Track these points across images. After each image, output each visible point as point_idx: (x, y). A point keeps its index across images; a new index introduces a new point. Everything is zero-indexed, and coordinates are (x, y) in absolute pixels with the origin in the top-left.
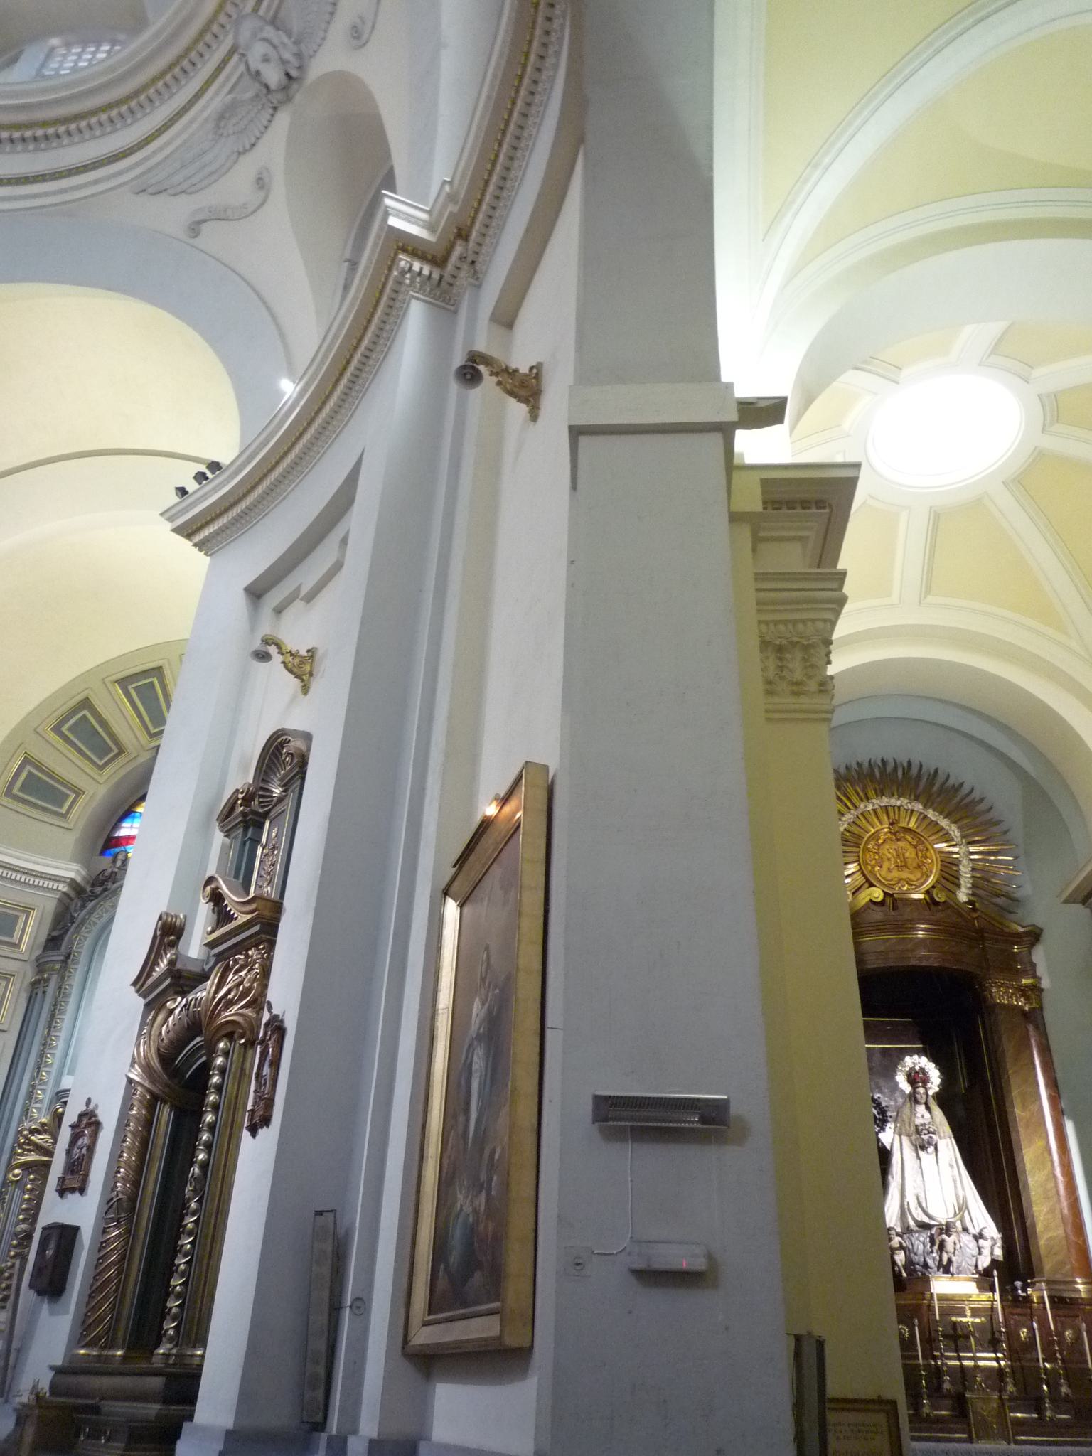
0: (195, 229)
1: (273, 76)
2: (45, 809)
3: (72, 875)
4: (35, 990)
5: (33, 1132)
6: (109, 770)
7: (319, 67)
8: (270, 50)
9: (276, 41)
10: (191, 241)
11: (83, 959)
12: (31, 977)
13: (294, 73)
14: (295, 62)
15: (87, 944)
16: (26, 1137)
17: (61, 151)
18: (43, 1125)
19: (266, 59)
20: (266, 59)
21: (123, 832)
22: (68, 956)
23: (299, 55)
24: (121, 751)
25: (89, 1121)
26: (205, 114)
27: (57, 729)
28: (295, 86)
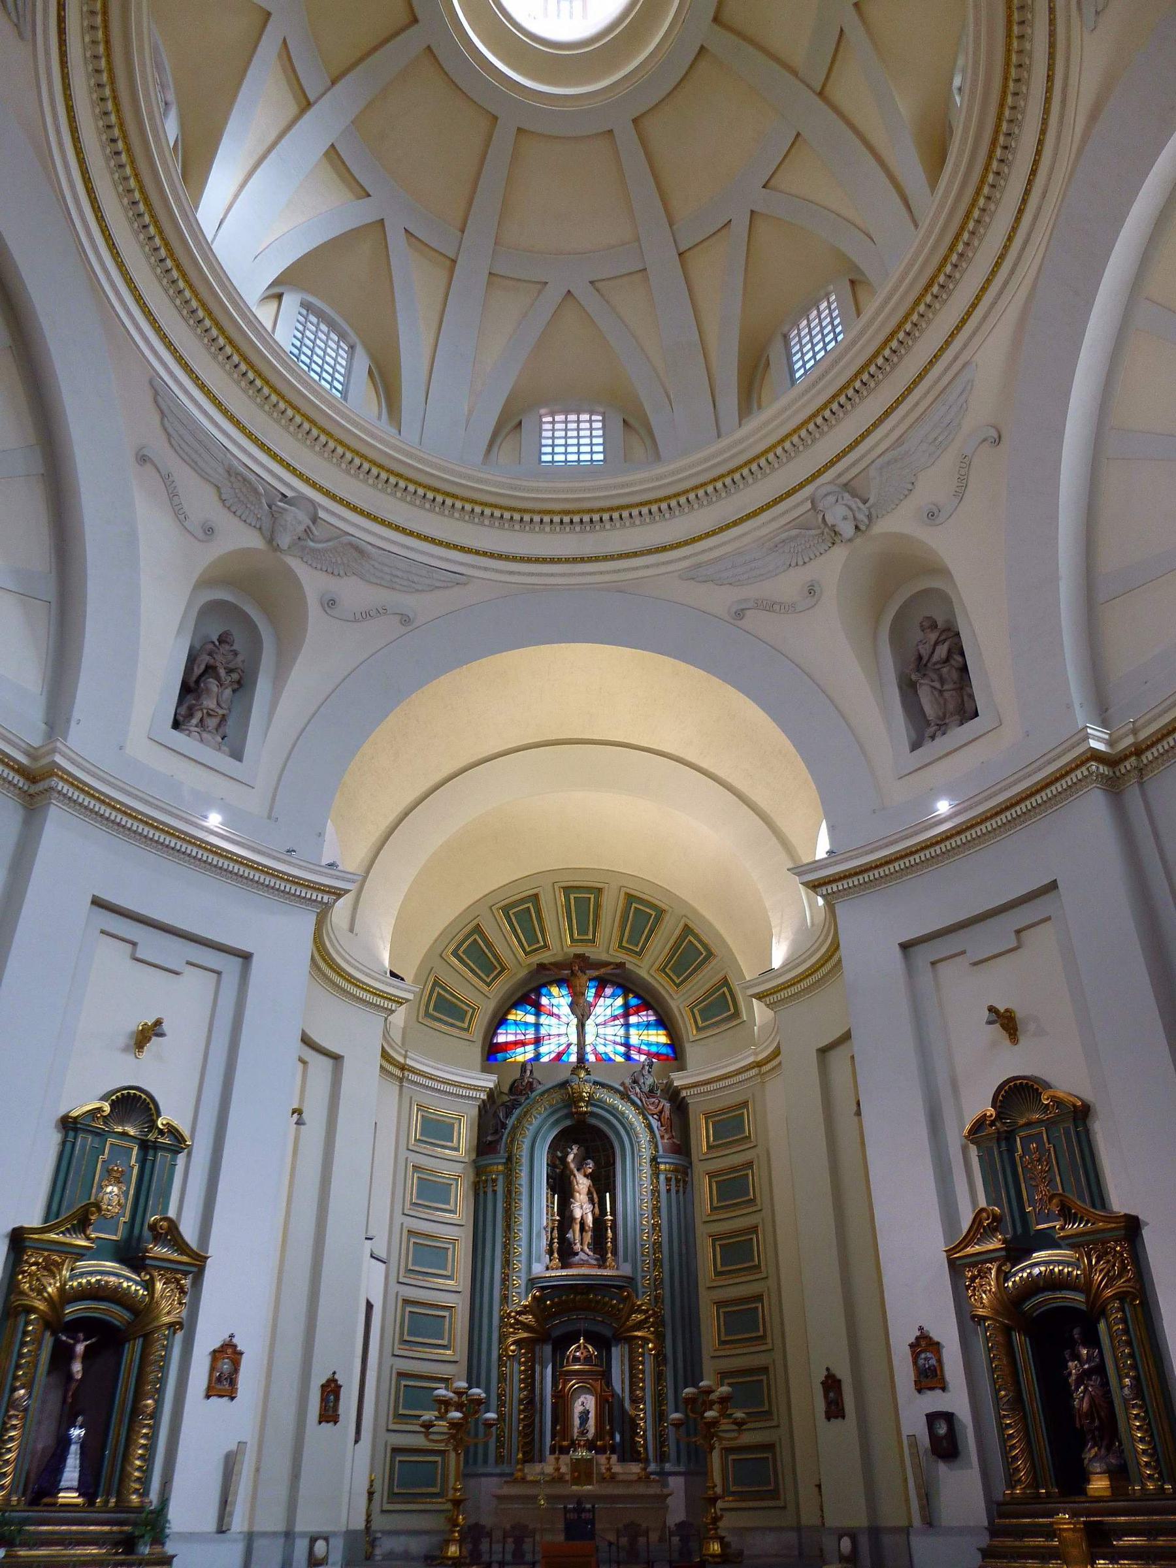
0: (740, 614)
1: (847, 530)
2: (452, 1025)
3: (491, 1085)
4: (480, 1189)
5: (519, 1313)
6: (495, 985)
7: (886, 525)
9: (854, 507)
10: (739, 623)
11: (525, 1161)
12: (471, 1176)
13: (863, 527)
14: (866, 520)
15: (526, 1147)
16: (514, 1318)
17: (605, 533)
18: (525, 1307)
19: (845, 518)
20: (845, 518)
21: (501, 1039)
22: (509, 1159)
23: (869, 517)
24: (503, 969)
25: (924, 1344)
26: (759, 533)
27: (455, 953)
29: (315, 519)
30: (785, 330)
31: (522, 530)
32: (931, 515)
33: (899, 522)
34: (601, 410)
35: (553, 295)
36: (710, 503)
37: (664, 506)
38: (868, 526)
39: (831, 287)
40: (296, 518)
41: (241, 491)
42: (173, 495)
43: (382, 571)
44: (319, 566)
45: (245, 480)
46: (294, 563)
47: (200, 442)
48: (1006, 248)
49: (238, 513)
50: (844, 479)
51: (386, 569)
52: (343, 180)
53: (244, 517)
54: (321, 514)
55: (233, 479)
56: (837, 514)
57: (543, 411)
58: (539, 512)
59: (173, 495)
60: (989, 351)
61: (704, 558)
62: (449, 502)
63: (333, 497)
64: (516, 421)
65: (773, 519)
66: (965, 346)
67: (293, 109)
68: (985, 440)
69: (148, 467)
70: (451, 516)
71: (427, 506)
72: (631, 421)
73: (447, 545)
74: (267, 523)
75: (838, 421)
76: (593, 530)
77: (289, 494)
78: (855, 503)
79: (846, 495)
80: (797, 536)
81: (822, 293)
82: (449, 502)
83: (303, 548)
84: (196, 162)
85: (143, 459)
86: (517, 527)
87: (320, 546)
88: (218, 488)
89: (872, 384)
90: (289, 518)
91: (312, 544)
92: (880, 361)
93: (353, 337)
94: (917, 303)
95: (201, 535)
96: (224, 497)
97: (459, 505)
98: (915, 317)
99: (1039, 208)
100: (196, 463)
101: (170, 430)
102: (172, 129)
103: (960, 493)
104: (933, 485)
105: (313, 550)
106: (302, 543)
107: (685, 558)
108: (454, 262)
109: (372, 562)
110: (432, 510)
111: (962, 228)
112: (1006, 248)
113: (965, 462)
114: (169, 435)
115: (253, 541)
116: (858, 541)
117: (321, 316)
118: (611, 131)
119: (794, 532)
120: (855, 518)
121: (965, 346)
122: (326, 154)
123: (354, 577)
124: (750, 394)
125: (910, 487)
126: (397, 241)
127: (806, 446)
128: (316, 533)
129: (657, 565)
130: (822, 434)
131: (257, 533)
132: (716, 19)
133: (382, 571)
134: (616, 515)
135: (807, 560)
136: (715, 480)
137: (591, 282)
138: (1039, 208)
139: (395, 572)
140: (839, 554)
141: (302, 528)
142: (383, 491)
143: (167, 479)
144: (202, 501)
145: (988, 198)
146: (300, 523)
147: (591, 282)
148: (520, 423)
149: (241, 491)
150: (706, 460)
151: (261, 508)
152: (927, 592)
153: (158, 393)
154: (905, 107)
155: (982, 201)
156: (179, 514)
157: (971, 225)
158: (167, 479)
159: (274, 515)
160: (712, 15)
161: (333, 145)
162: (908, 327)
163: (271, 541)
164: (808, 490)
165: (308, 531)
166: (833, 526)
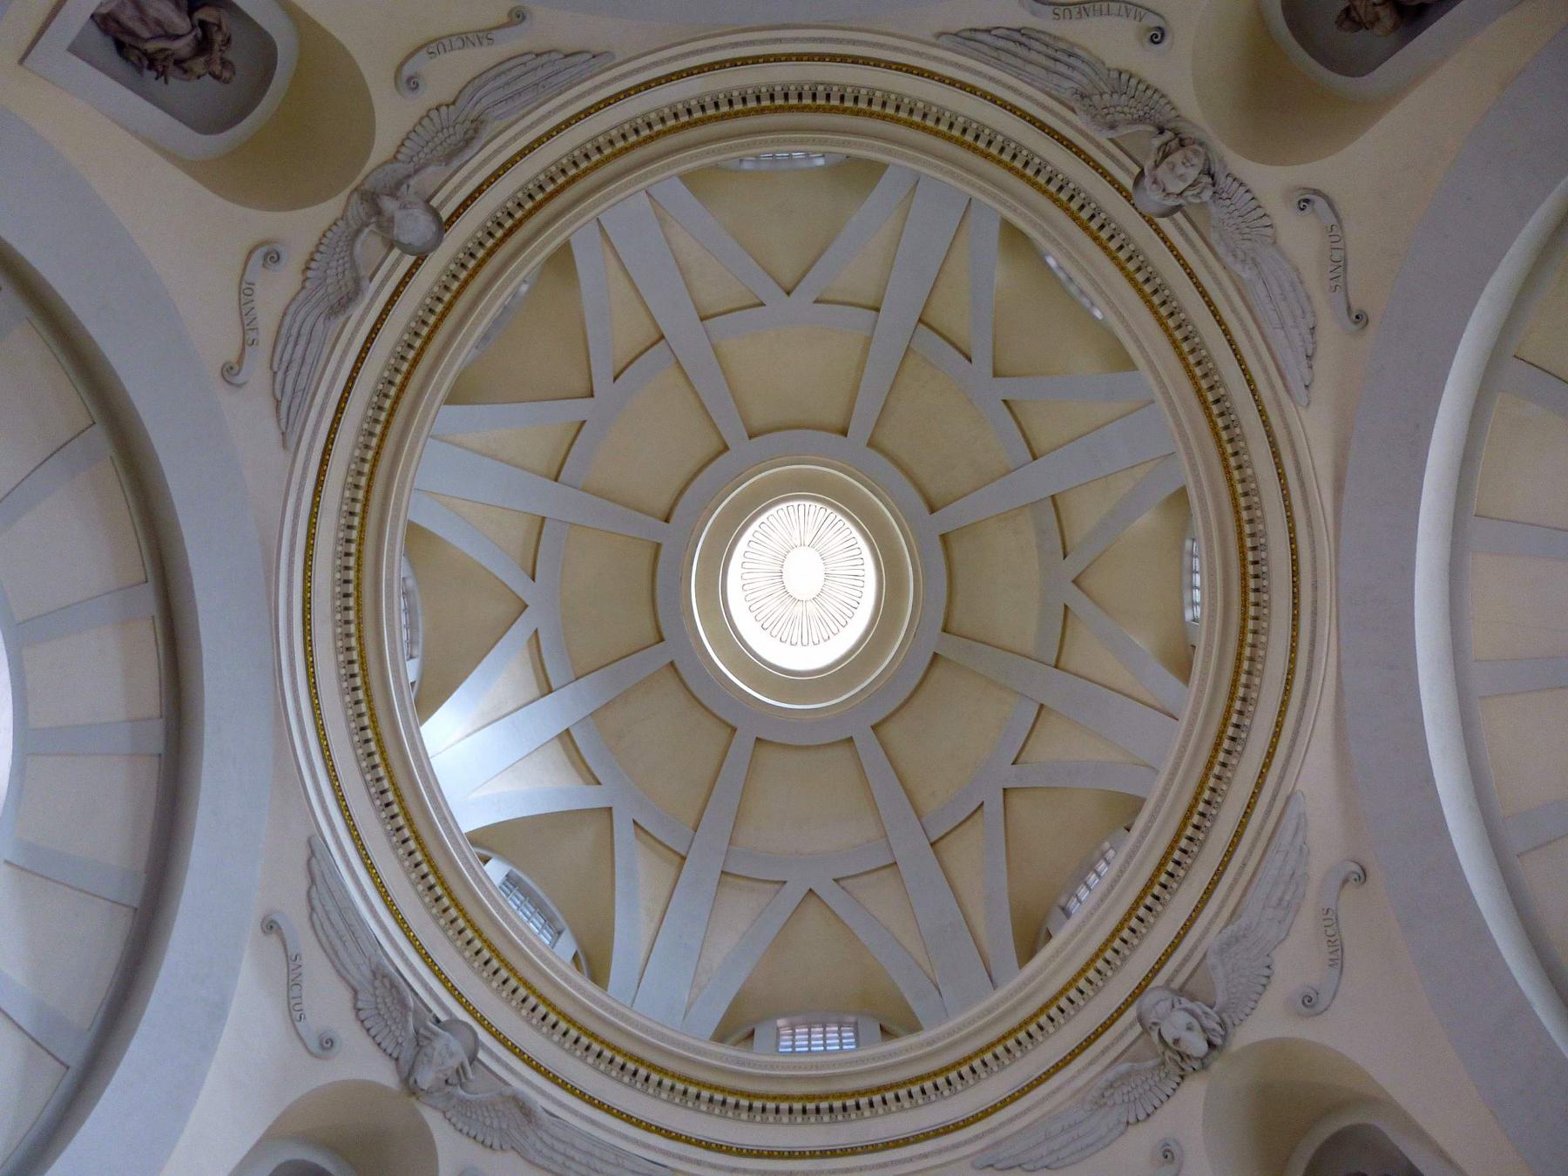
7: (1245, 1036)
8: (1189, 1019)
9: (1199, 1011)
13: (1218, 1041)
19: (1189, 1028)
23: (1222, 1024)
26: (1080, 1082)
28: (1215, 1053)
29: (473, 1058)
30: (1062, 901)
31: (751, 1120)
32: (1308, 1001)
33: (1265, 1024)
34: (852, 1019)
35: (795, 892)
36: (1002, 1067)
37: (941, 1081)
38: (1224, 1037)
39: (1107, 845)
40: (447, 1050)
41: (383, 1000)
42: (294, 981)
43: (552, 1148)
44: (465, 1129)
45: (393, 985)
46: (433, 1119)
47: (349, 926)
48: (1292, 661)
49: (373, 1032)
50: (1176, 985)
51: (560, 1147)
52: (573, 763)
53: (378, 1039)
54: (481, 1055)
55: (377, 983)
56: (1176, 1024)
57: (781, 1022)
58: (774, 1098)
59: (294, 981)
60: (1313, 773)
61: (1002, 1133)
62: (655, 1077)
63: (504, 1041)
64: (750, 1028)
65: (1091, 1063)
66: (1281, 778)
67: (535, 692)
68: (1346, 881)
69: (274, 938)
70: (656, 1097)
71: (626, 1079)
72: (888, 1025)
73: (648, 1127)
74: (407, 1053)
75: (1150, 927)
76: (847, 1120)
77: (443, 1017)
78: (1197, 1007)
79: (1186, 1003)
80: (1128, 1074)
81: (1097, 854)
82: (655, 1077)
83: (449, 1096)
84: (429, 699)
85: (270, 926)
86: (744, 1116)
87: (468, 1096)
88: (355, 992)
89: (1181, 873)
90: (438, 1045)
91: (462, 1093)
92: (1183, 843)
93: (561, 922)
94: (1209, 766)
95: (314, 1045)
96: (360, 1005)
97: (667, 1082)
98: (1212, 782)
99: (1315, 602)
100: (336, 953)
101: (316, 902)
102: (412, 670)
103: (1337, 960)
104: (1296, 962)
105: (463, 1101)
106: (449, 1089)
107: (977, 1138)
108: (684, 858)
109: (540, 1133)
110: (631, 1086)
111: (1237, 673)
112: (1292, 661)
113: (1329, 917)
114: (313, 909)
115: (384, 1075)
116: (1216, 1066)
117: (528, 894)
118: (850, 740)
119: (1123, 1067)
120: (1204, 1030)
121: (1281, 778)
122: (559, 736)
123: (512, 1155)
124: (1030, 940)
125: (1267, 972)
126: (623, 833)
127: (1115, 970)
128: (470, 1076)
129: (940, 1152)
130: (1133, 948)
131: (391, 1065)
132: (944, 630)
133: (552, 1148)
134: (877, 1098)
135: (1150, 1110)
136: (1004, 1038)
137: (836, 880)
138: (1315, 602)
139: (572, 1153)
140: (1195, 1090)
141: (453, 1063)
142: (570, 1052)
143: (293, 963)
144: (329, 1003)
145: (1254, 646)
146: (452, 1055)
147: (836, 880)
148: (751, 1035)
149: (383, 1000)
150: (989, 1011)
151: (405, 1028)
152: (1337, 1140)
153: (314, 851)
154: (1144, 642)
155: (1250, 638)
156: (294, 1011)
157: (1246, 665)
158: (293, 963)
159: (421, 1040)
160: (941, 625)
161: (567, 730)
162: (1206, 795)
163: (410, 1087)
164: (1131, 1013)
165: (460, 1071)
166: (1176, 1041)
